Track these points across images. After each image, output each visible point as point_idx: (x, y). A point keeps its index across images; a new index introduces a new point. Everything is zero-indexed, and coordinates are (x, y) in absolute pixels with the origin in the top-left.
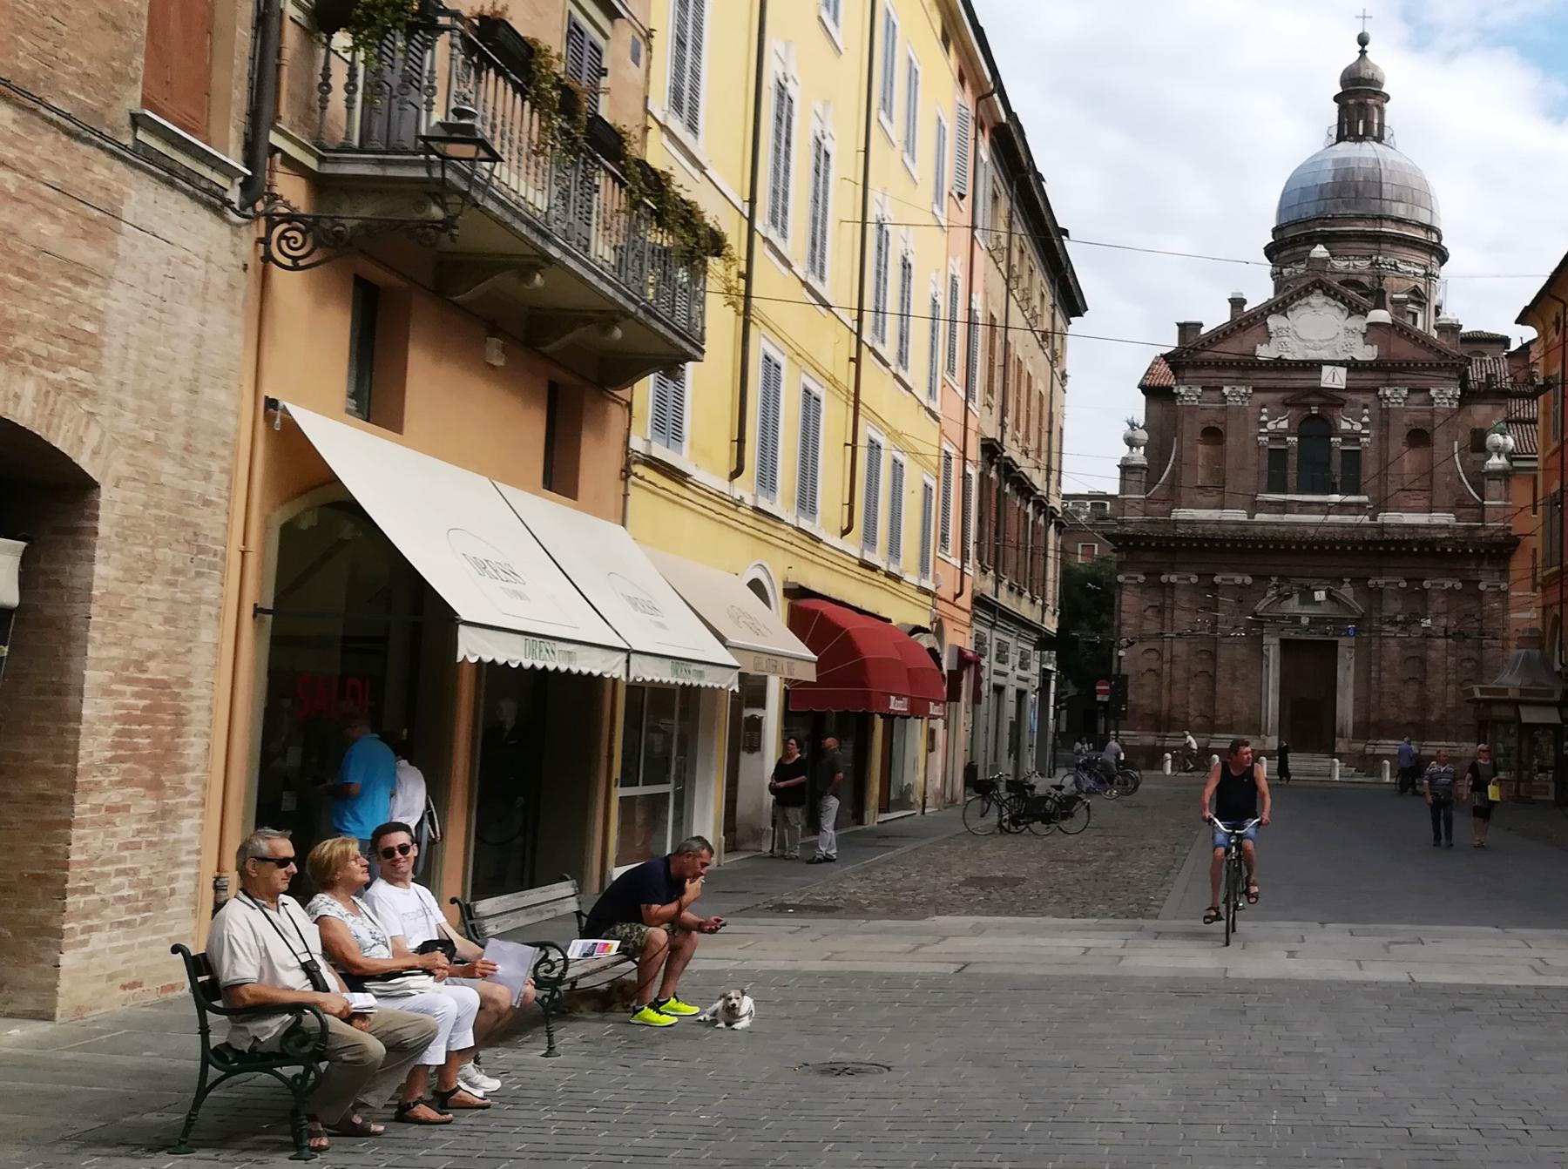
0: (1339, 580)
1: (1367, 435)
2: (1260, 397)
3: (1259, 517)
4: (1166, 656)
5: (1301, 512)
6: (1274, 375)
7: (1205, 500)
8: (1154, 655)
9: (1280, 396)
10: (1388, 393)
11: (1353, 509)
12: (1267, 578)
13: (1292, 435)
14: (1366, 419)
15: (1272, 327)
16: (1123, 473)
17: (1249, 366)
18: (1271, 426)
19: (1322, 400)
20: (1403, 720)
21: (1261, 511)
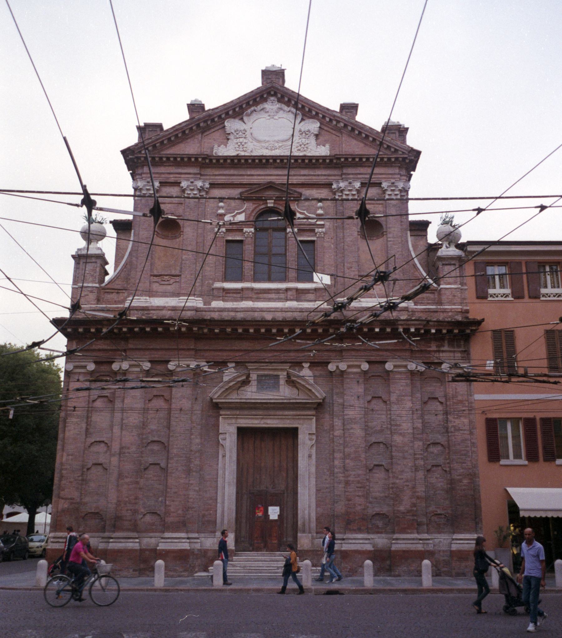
0: (298, 364)
1: (322, 226)
2: (217, 193)
3: (216, 304)
4: (116, 447)
5: (258, 299)
6: (232, 172)
7: (161, 288)
8: (101, 448)
9: (236, 192)
10: (342, 185)
11: (311, 296)
12: (223, 364)
13: (249, 226)
14: (320, 212)
15: (228, 130)
16: (77, 263)
17: (208, 162)
18: (227, 218)
19: (277, 194)
20: (370, 512)
21: (217, 298)
